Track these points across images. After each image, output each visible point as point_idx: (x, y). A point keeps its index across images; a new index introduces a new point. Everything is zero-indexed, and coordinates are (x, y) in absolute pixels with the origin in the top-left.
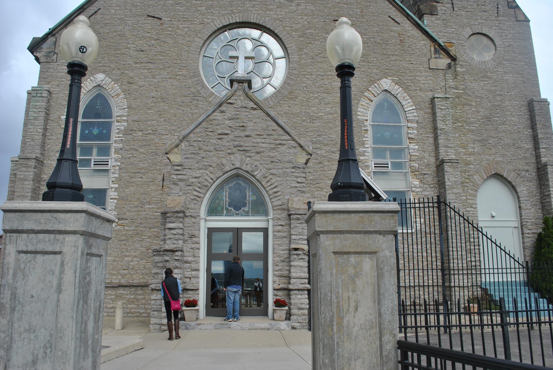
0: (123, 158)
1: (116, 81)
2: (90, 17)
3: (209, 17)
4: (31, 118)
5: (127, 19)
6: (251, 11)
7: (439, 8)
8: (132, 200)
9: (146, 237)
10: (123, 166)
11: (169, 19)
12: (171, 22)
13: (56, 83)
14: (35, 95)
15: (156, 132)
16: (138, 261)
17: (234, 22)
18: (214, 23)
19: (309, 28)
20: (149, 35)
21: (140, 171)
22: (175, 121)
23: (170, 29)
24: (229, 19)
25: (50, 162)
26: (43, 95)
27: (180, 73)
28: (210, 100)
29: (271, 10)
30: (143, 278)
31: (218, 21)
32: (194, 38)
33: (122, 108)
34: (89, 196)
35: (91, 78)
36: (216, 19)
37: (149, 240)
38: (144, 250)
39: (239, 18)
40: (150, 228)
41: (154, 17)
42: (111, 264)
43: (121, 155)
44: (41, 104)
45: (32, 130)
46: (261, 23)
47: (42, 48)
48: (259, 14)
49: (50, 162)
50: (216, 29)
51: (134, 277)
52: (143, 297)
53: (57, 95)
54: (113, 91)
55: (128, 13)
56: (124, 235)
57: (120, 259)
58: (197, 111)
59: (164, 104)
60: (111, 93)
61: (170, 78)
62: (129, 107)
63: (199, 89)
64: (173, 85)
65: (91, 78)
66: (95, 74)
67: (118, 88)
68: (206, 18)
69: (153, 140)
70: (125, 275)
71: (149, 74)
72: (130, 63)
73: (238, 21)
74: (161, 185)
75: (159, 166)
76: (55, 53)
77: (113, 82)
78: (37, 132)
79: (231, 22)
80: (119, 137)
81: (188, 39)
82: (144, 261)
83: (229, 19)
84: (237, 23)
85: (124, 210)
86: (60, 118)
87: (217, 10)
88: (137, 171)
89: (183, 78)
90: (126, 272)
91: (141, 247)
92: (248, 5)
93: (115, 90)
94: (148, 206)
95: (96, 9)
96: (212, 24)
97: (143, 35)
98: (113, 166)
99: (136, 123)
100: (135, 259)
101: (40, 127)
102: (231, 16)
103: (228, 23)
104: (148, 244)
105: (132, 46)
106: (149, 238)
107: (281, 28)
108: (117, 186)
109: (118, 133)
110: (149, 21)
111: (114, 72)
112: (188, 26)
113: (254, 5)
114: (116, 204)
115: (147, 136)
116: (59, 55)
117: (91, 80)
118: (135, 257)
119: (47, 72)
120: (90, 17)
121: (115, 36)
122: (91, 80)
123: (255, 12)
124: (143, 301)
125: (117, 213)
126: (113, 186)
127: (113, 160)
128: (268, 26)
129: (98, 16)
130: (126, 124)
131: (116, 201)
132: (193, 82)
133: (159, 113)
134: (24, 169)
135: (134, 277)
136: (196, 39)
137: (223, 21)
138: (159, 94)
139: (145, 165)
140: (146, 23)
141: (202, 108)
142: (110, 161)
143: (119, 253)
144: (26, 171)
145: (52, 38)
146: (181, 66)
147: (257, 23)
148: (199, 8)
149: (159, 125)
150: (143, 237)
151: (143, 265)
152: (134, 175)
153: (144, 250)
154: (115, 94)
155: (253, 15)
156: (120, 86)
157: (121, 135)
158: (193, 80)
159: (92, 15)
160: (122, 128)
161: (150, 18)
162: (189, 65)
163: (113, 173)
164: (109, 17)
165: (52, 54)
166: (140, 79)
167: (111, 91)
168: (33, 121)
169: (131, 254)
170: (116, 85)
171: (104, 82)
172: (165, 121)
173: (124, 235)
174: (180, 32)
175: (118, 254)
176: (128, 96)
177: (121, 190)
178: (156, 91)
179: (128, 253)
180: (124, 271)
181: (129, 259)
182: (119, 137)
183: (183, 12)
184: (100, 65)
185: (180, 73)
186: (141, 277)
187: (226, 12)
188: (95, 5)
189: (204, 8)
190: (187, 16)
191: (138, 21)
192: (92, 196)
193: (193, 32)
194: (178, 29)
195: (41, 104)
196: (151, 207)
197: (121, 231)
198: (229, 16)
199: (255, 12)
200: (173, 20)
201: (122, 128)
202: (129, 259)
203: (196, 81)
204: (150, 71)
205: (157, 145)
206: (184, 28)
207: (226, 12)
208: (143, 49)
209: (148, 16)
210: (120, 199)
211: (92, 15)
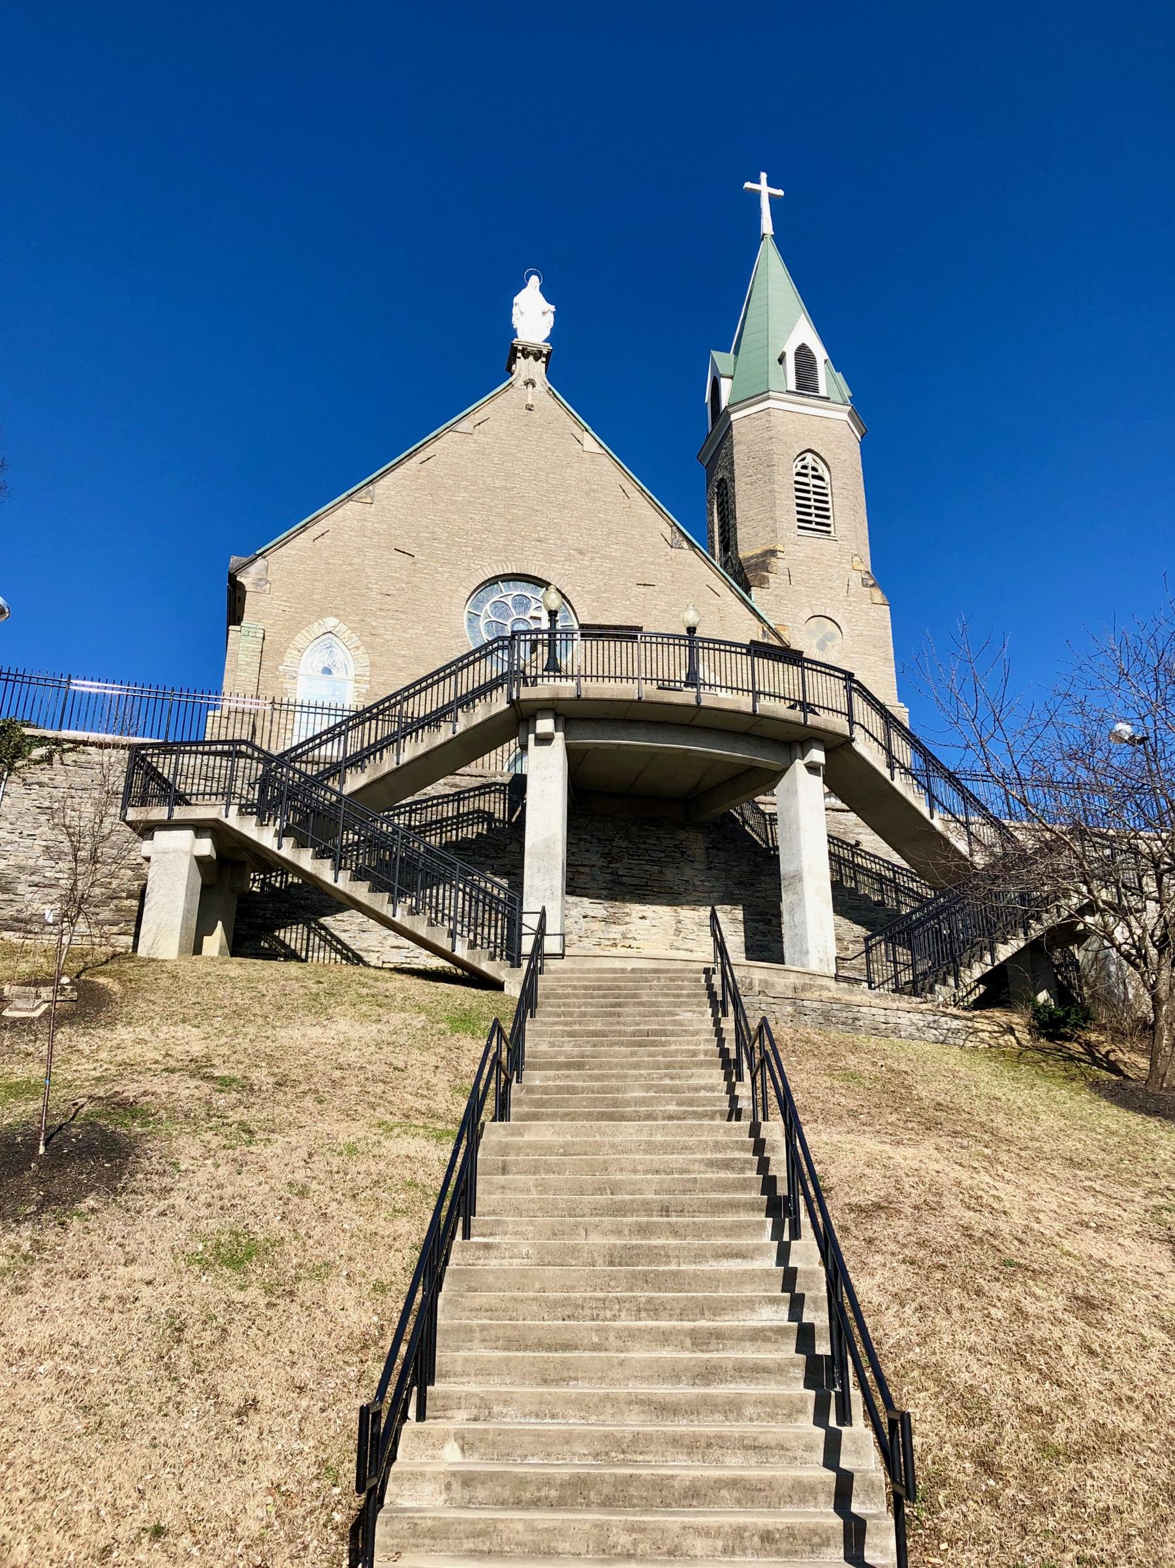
1: (353, 630)
7: (771, 580)
19: (606, 591)
29: (557, 562)
48: (541, 566)
62: (373, 665)
84: (513, 574)
86: (277, 668)
107: (570, 587)
109: (358, 696)
129: (325, 540)
130: (368, 687)
136: (461, 588)
160: (364, 691)
174: (438, 577)
201: (364, 691)
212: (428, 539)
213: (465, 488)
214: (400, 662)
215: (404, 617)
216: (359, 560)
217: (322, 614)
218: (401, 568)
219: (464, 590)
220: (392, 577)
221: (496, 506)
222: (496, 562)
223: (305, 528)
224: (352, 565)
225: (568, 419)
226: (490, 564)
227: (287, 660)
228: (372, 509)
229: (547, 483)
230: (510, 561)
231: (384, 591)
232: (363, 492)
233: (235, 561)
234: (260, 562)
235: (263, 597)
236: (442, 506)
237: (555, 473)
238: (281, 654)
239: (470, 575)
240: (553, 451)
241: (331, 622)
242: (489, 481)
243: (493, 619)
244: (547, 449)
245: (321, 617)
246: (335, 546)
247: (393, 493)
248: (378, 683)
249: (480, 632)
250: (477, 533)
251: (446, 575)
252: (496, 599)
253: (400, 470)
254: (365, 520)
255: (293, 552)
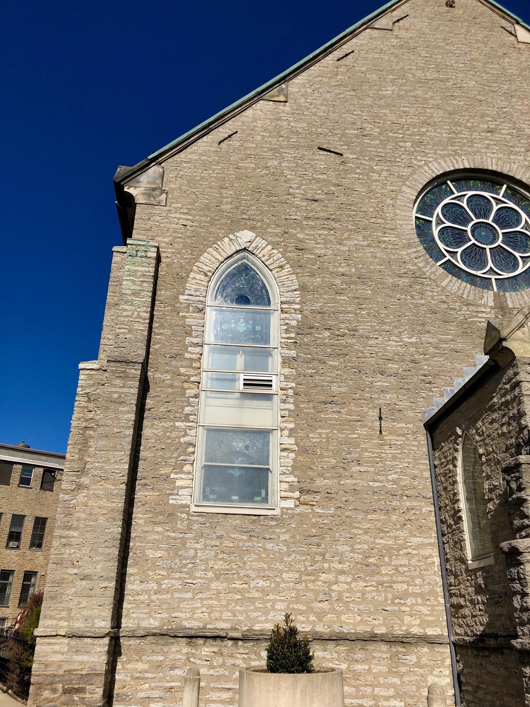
0: (299, 375)
1: (275, 245)
2: (220, 143)
3: (419, 158)
4: (128, 292)
5: (284, 151)
6: (486, 153)
8: (325, 453)
9: (361, 532)
10: (301, 388)
11: (355, 156)
12: (359, 162)
13: (166, 240)
14: (134, 252)
15: (356, 333)
16: (349, 584)
17: (462, 167)
18: (429, 167)
20: (325, 177)
21: (335, 399)
22: (387, 316)
23: (358, 171)
24: (452, 162)
25: (159, 375)
26: (149, 254)
27: (385, 239)
28: (444, 284)
29: (517, 153)
30: (362, 620)
31: (436, 165)
32: (400, 187)
33: (290, 289)
34: (235, 444)
35: (231, 236)
36: (431, 162)
37: (366, 537)
38: (359, 557)
39: (469, 163)
40: (367, 512)
41: (329, 151)
42: (294, 589)
43: (296, 369)
44: (146, 269)
45: (129, 313)
46: (505, 172)
47: (139, 182)
48: (499, 159)
49: (159, 375)
50: (434, 176)
51: (343, 618)
52: (367, 667)
53: (169, 260)
54: (271, 261)
55: (286, 143)
56: (314, 525)
57: (312, 578)
58: (423, 302)
59: (363, 287)
60: (267, 263)
61: (369, 246)
63: (421, 265)
64: (376, 257)
65: (231, 236)
66: (237, 232)
67: (281, 256)
68: (415, 159)
69: (352, 345)
70: (325, 613)
71: (332, 238)
72: (296, 217)
73: (468, 166)
74: (378, 429)
75: (368, 392)
76: (163, 191)
77: (270, 247)
78: (139, 316)
79: (457, 167)
80: (288, 338)
81: (392, 188)
82: (361, 584)
83: (452, 162)
84: (465, 170)
85: (310, 473)
86: (177, 298)
87: (430, 149)
88: (330, 399)
89: (390, 246)
90: (325, 606)
91: (353, 551)
92: (480, 145)
93: (275, 258)
94: (358, 468)
95: (231, 133)
96: (426, 168)
97: (314, 175)
98: (282, 389)
99: (319, 316)
100: (342, 578)
101: (145, 309)
102: (455, 159)
103: (452, 169)
104: (366, 547)
105: (298, 191)
106: (366, 532)
108: (292, 426)
109: (287, 331)
110: (322, 157)
111: (269, 230)
112: (388, 168)
113: (489, 145)
114: (294, 460)
115: (339, 338)
116: (170, 196)
117: (231, 240)
118: (342, 572)
119: (149, 219)
120: (220, 143)
121: (267, 175)
122: (231, 240)
123: (492, 156)
124: (370, 678)
125: (296, 479)
126: (284, 425)
127: (282, 378)
128: (518, 177)
129: (234, 142)
130: (299, 316)
131: (292, 455)
132: (408, 254)
133: (357, 301)
134: (118, 382)
135: (343, 618)
136: (404, 188)
137: (443, 164)
138: (354, 270)
139: (343, 390)
140: (317, 160)
141: (433, 297)
142: (274, 378)
143: (307, 564)
144: (124, 387)
145: (156, 167)
146: (384, 228)
147: (499, 170)
148: (402, 144)
149: (358, 321)
150: (354, 531)
151: (359, 591)
152: (323, 406)
153: (359, 557)
154: (275, 265)
155: (489, 160)
156: (284, 254)
157: (293, 335)
158: (409, 251)
159: (223, 141)
160: (294, 323)
161: (322, 152)
162: (399, 227)
163: (284, 401)
164: (254, 146)
165: (157, 192)
166: (317, 243)
167: (267, 260)
168: (130, 298)
169: (332, 565)
170: (275, 251)
171: (254, 245)
172: (368, 314)
173: (314, 525)
174: (375, 176)
175: (306, 567)
176: (298, 271)
177: (302, 434)
178: (348, 265)
179: (326, 565)
180: (320, 605)
181: (331, 577)
182: (288, 338)
183: (375, 148)
184: (244, 216)
185: (385, 239)
186: (358, 618)
187: (445, 152)
188: (227, 125)
189: (408, 144)
190: (383, 155)
191: (303, 155)
192: (241, 445)
193: (398, 177)
194: (374, 173)
195: (146, 269)
196: (362, 469)
197: (307, 515)
198: (452, 158)
199: (492, 156)
200: (361, 157)
201: (294, 323)
202: (331, 577)
203: (415, 252)
204: (332, 232)
205: (360, 355)
206: (382, 170)
207: (445, 152)
208: (317, 197)
209: (320, 148)
210: (303, 450)
211: (223, 141)
212: (357, 136)
213: (393, 82)
214: (338, 281)
215: (337, 225)
216: (275, 163)
217: (234, 226)
218: (328, 168)
219: (408, 190)
220: (318, 181)
221: (432, 98)
222: (443, 156)
223: (207, 130)
224: (267, 168)
225: (494, 15)
226: (435, 160)
227: (191, 286)
228: (287, 108)
229: (487, 73)
230: (460, 155)
231: (309, 196)
232: (275, 91)
233: (121, 170)
234: (154, 170)
235: (157, 210)
236: (369, 101)
237: (492, 63)
238: (182, 280)
239: (414, 173)
240: (485, 44)
241: (245, 236)
242: (419, 74)
243: (448, 224)
244: (478, 41)
245: (233, 231)
246: (246, 149)
247: (309, 91)
248: (313, 312)
249: (433, 240)
250: (415, 127)
251: (384, 174)
252: (447, 201)
253: (315, 69)
254: (280, 119)
255: (194, 157)
